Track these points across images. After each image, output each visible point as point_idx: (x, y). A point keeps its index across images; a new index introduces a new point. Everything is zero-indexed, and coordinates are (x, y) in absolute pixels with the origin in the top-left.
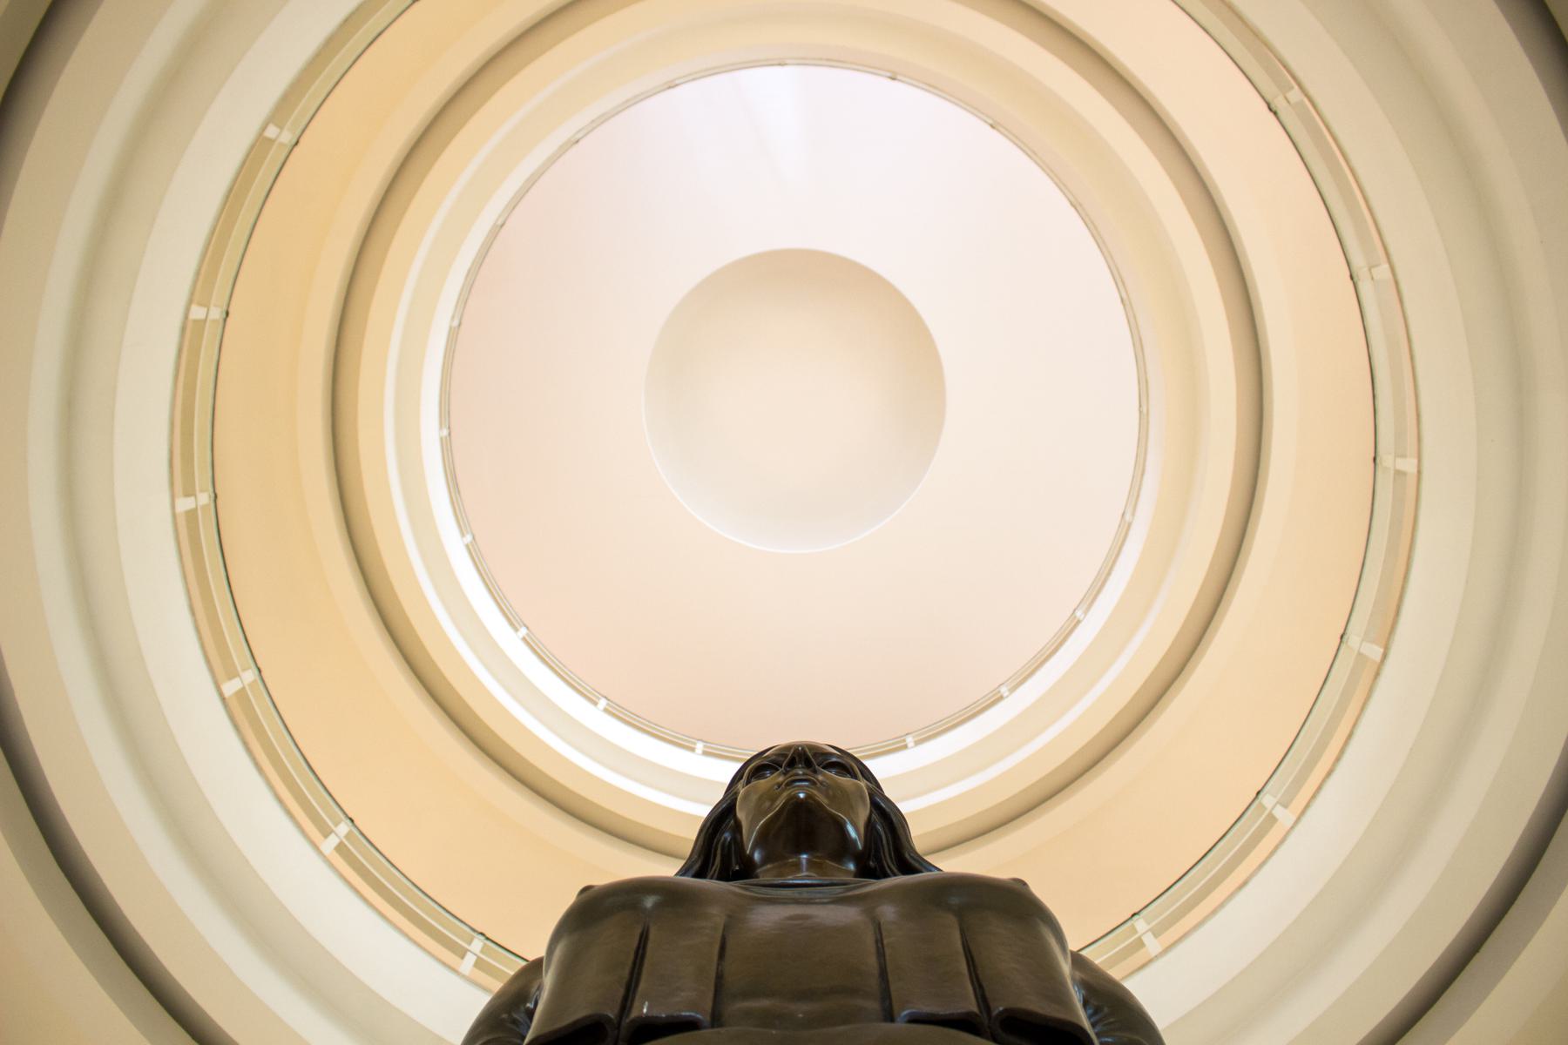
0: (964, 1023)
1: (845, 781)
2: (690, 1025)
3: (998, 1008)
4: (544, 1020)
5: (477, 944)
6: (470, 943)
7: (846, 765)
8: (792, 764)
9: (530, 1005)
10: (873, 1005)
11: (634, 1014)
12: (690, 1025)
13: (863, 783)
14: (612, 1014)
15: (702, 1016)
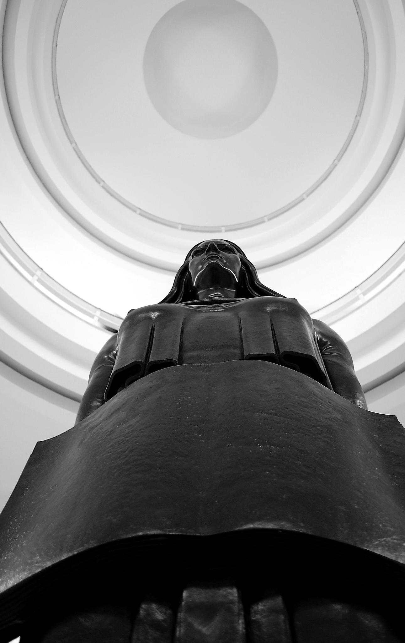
0: (269, 358)
1: (231, 255)
2: (168, 364)
3: (281, 351)
4: (119, 363)
5: (98, 313)
6: (95, 312)
7: (232, 248)
8: (209, 250)
9: (115, 352)
10: (237, 351)
11: (150, 360)
12: (168, 364)
13: (238, 255)
14: (143, 360)
15: (175, 357)
